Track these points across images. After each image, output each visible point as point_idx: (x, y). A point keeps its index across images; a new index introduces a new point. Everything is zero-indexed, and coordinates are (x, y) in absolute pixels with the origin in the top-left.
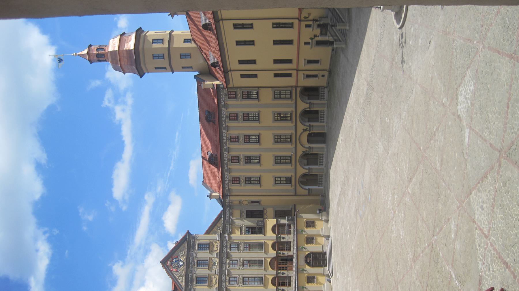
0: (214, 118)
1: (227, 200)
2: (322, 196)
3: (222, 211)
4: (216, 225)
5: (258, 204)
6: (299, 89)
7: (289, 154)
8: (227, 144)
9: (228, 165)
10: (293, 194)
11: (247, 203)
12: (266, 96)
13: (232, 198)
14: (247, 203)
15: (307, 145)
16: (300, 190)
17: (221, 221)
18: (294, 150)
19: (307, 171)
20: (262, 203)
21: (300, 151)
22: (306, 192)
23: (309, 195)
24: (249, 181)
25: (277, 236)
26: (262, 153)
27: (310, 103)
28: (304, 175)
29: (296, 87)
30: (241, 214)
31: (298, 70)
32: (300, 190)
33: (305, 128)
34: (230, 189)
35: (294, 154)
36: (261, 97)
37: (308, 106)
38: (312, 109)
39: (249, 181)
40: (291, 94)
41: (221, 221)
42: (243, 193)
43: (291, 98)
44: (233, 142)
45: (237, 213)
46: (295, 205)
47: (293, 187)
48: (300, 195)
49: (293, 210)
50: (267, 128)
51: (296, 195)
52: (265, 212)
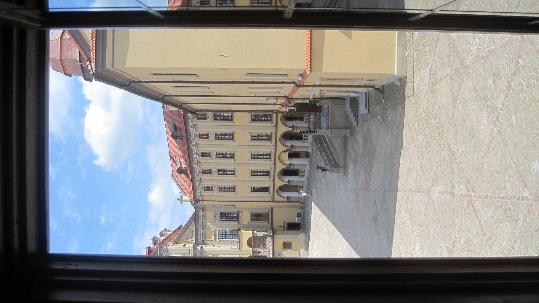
0: (181, 134)
1: (199, 204)
2: (301, 203)
3: (194, 213)
4: (188, 228)
8: (197, 158)
9: (198, 175)
10: (271, 199)
12: (242, 119)
13: (203, 203)
15: (288, 161)
16: (277, 198)
17: (194, 223)
18: (273, 166)
21: (280, 167)
22: (286, 200)
23: (288, 201)
24: (224, 189)
25: (253, 250)
26: (236, 168)
27: (293, 127)
30: (215, 217)
32: (277, 198)
33: (285, 149)
37: (291, 129)
38: (295, 131)
39: (224, 189)
41: (194, 223)
42: (217, 200)
44: (203, 138)
45: (210, 215)
46: (272, 209)
48: (278, 202)
50: (243, 146)
52: (240, 214)
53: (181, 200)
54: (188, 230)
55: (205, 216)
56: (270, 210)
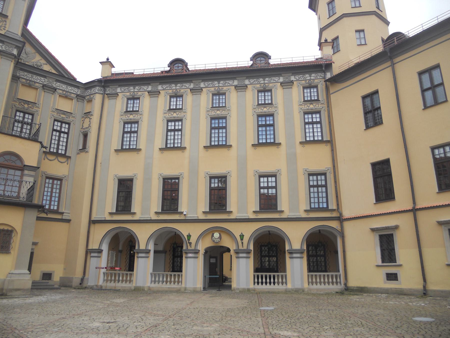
5: (81, 147)
6: (334, 224)
7: (183, 207)
8: (208, 88)
11: (86, 125)
13: (98, 99)
14: (86, 125)
15: (202, 247)
19: (142, 247)
20: (83, 154)
22: (94, 245)
23: (88, 252)
28: (131, 241)
29: (340, 219)
30: (64, 112)
31: (414, 211)
34: (117, 94)
35: (182, 217)
36: (310, 148)
40: (319, 210)
43: (312, 210)
45: (66, 105)
46: (68, 221)
47: (108, 218)
49: (59, 217)
51: (92, 222)
53: (107, 63)
54: (43, 61)
55: (66, 97)
56: (64, 217)
